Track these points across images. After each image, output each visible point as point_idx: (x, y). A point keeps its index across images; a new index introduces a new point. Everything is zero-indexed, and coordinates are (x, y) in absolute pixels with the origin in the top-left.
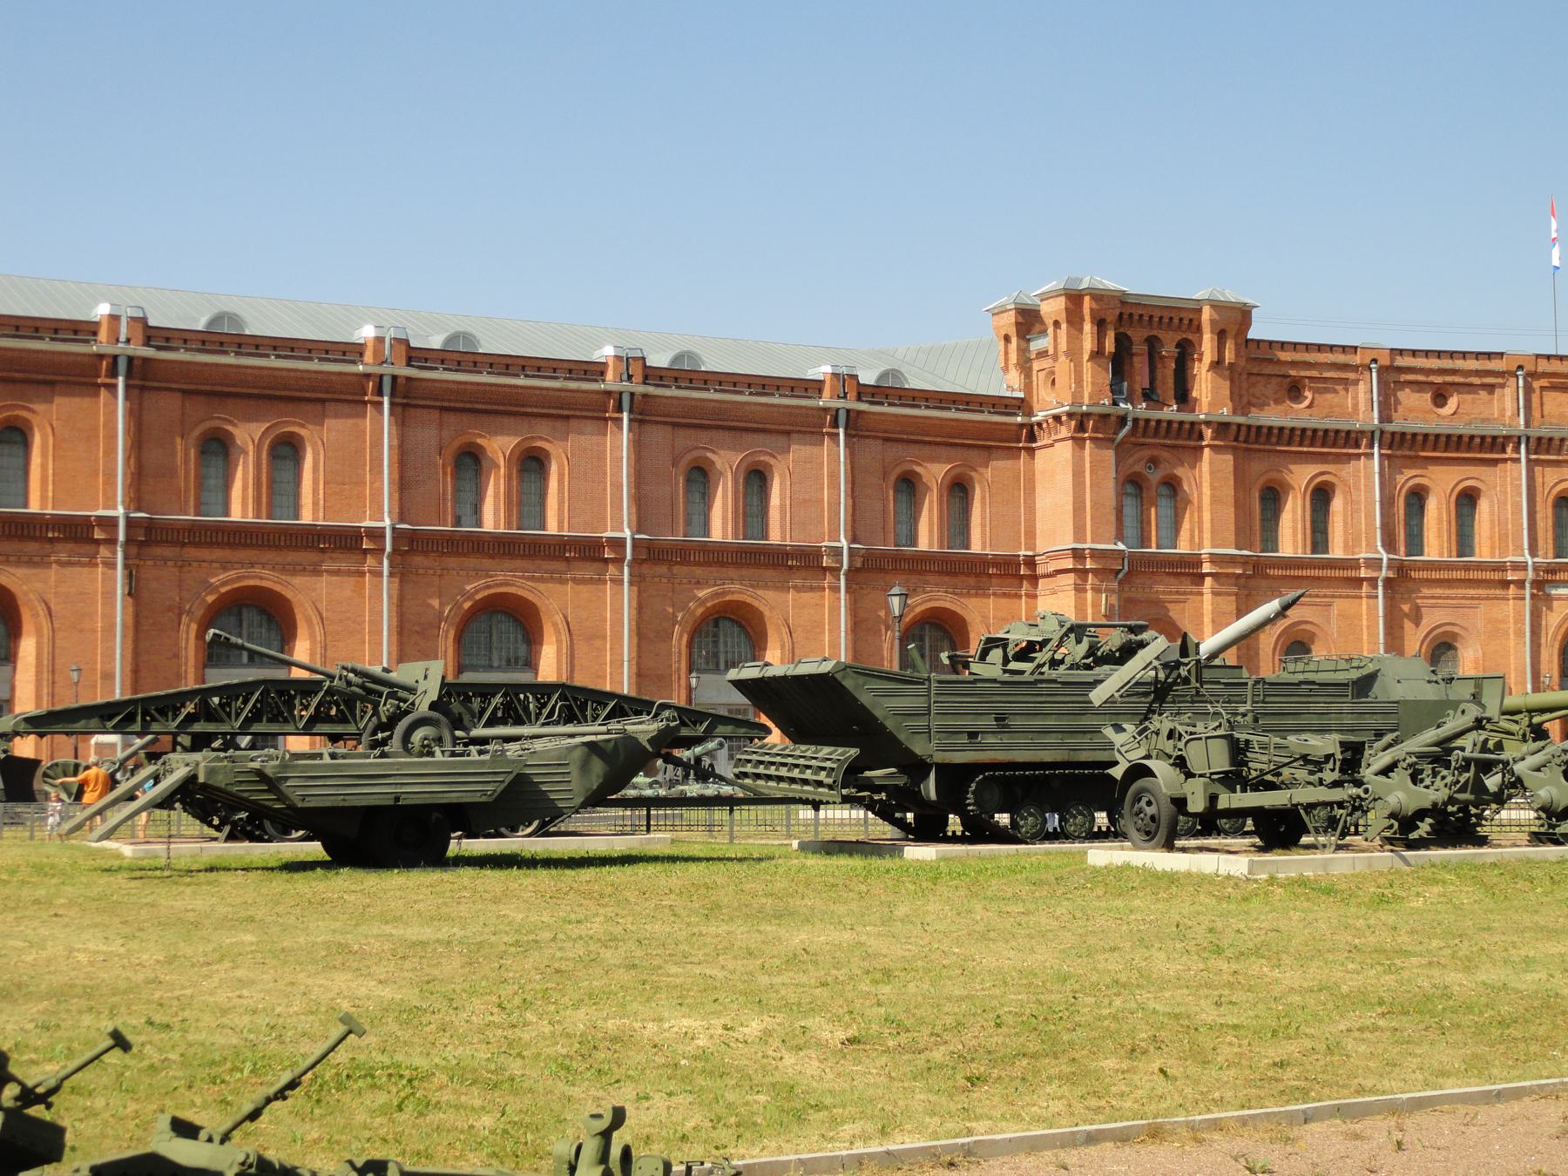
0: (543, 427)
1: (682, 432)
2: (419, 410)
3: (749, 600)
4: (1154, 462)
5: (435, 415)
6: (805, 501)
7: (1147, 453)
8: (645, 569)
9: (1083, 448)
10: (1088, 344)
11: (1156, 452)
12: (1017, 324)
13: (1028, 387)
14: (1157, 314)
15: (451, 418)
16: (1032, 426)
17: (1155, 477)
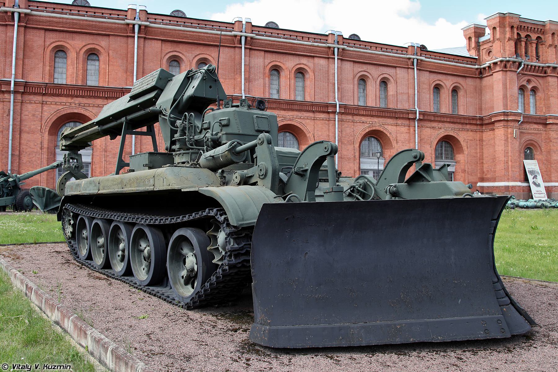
0: (304, 61)
1: (357, 65)
2: (256, 52)
3: (382, 130)
4: (529, 81)
5: (263, 53)
6: (402, 93)
7: (527, 78)
8: (344, 117)
9: (506, 75)
10: (508, 35)
11: (530, 78)
12: (475, 32)
13: (479, 55)
14: (530, 26)
15: (269, 55)
16: (481, 69)
17: (529, 87)
